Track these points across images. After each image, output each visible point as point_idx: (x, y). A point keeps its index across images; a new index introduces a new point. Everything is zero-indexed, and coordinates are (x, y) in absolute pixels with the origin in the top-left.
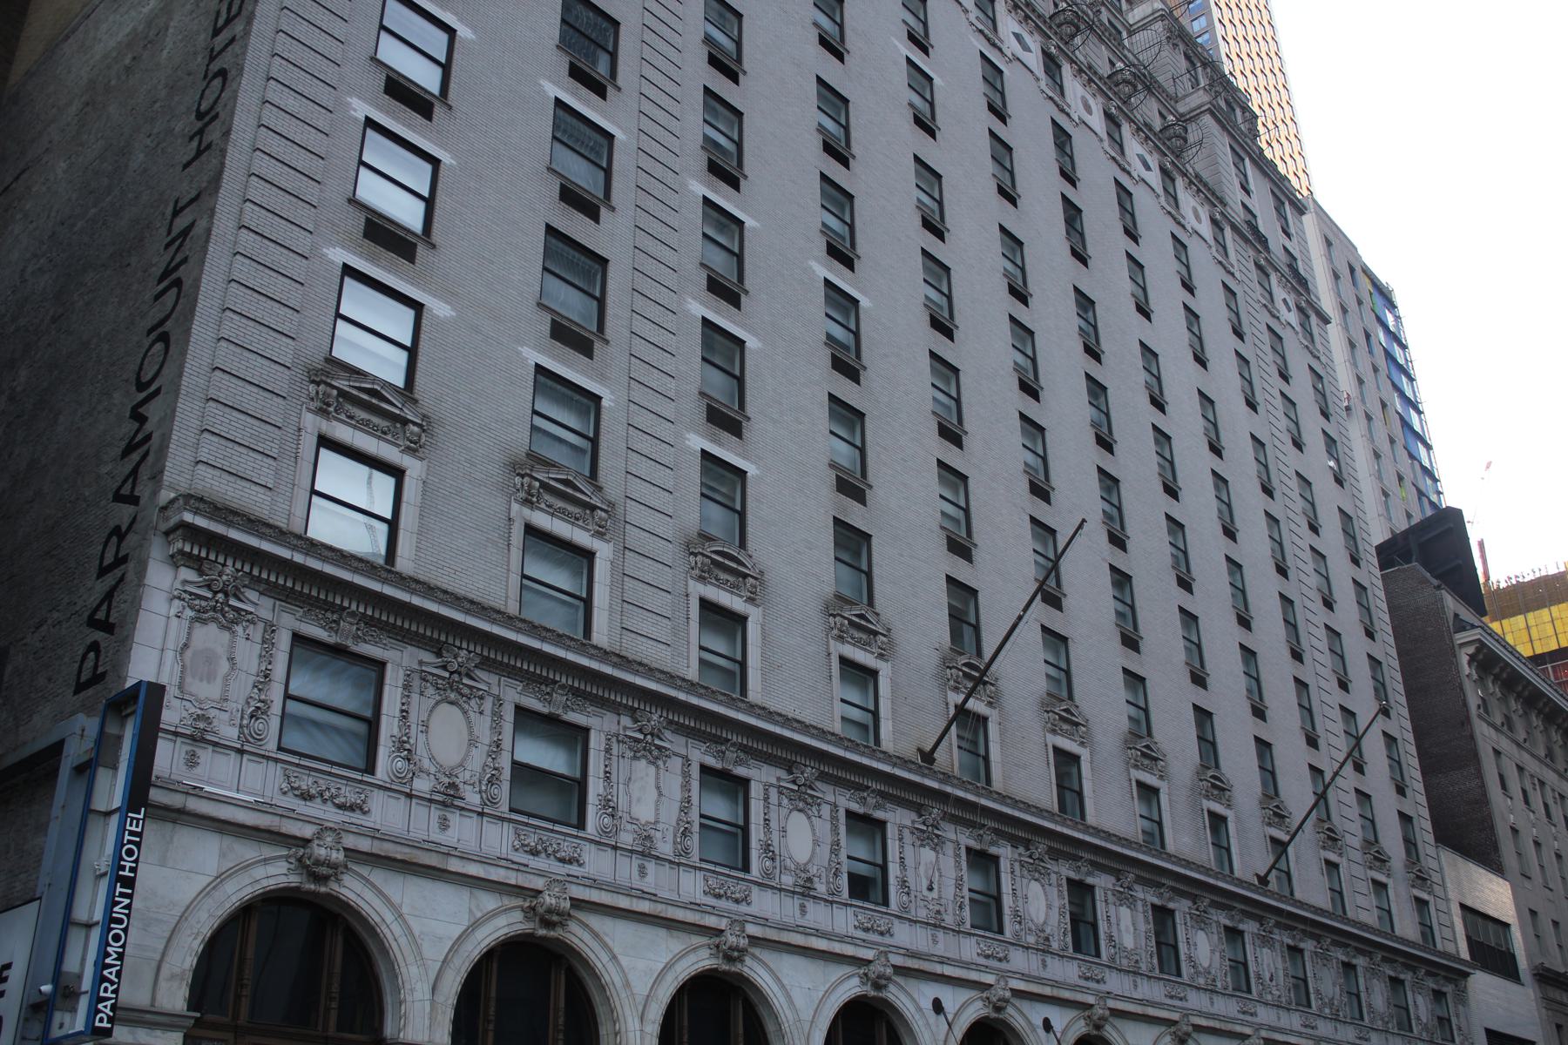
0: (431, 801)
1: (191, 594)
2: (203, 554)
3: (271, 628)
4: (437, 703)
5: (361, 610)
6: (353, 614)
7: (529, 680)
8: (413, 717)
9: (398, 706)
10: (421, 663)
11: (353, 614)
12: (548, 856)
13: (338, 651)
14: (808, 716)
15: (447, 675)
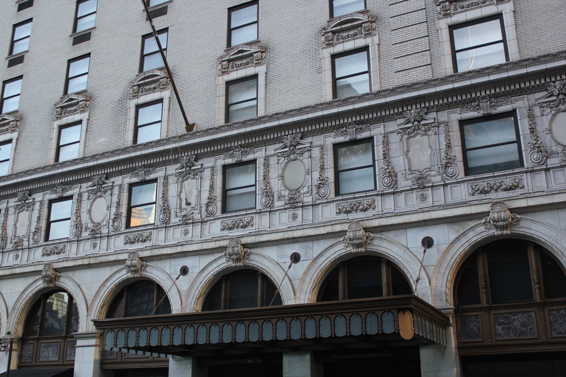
0: (285, 209)
1: (403, 129)
2: (543, 81)
3: (446, 124)
4: (554, 116)
5: (436, 103)
6: (484, 98)
7: (463, 104)
8: (539, 128)
9: (528, 127)
10: (536, 100)
11: (484, 98)
12: (237, 227)
13: (488, 118)
14: (311, 102)
15: (555, 98)
